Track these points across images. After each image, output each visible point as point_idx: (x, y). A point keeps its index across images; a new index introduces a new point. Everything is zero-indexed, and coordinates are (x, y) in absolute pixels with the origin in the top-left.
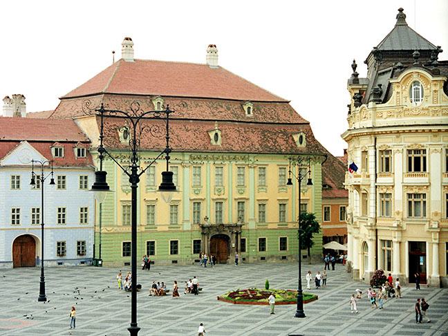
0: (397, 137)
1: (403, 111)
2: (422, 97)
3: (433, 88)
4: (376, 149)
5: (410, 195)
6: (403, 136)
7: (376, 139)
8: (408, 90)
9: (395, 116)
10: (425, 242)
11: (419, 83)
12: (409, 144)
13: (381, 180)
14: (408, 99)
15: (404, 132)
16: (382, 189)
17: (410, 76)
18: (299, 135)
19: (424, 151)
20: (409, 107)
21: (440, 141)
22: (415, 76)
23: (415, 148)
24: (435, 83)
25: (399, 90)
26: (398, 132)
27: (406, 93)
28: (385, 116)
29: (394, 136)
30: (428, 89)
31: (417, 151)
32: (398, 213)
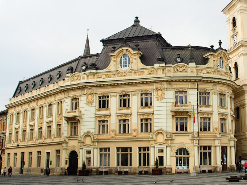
1: (215, 70)
4: (197, 90)
5: (220, 118)
6: (217, 85)
7: (197, 84)
9: (212, 73)
10: (226, 147)
13: (200, 109)
20: (219, 70)
23: (223, 93)
28: (204, 71)
29: (212, 84)
30: (225, 63)
32: (216, 129)
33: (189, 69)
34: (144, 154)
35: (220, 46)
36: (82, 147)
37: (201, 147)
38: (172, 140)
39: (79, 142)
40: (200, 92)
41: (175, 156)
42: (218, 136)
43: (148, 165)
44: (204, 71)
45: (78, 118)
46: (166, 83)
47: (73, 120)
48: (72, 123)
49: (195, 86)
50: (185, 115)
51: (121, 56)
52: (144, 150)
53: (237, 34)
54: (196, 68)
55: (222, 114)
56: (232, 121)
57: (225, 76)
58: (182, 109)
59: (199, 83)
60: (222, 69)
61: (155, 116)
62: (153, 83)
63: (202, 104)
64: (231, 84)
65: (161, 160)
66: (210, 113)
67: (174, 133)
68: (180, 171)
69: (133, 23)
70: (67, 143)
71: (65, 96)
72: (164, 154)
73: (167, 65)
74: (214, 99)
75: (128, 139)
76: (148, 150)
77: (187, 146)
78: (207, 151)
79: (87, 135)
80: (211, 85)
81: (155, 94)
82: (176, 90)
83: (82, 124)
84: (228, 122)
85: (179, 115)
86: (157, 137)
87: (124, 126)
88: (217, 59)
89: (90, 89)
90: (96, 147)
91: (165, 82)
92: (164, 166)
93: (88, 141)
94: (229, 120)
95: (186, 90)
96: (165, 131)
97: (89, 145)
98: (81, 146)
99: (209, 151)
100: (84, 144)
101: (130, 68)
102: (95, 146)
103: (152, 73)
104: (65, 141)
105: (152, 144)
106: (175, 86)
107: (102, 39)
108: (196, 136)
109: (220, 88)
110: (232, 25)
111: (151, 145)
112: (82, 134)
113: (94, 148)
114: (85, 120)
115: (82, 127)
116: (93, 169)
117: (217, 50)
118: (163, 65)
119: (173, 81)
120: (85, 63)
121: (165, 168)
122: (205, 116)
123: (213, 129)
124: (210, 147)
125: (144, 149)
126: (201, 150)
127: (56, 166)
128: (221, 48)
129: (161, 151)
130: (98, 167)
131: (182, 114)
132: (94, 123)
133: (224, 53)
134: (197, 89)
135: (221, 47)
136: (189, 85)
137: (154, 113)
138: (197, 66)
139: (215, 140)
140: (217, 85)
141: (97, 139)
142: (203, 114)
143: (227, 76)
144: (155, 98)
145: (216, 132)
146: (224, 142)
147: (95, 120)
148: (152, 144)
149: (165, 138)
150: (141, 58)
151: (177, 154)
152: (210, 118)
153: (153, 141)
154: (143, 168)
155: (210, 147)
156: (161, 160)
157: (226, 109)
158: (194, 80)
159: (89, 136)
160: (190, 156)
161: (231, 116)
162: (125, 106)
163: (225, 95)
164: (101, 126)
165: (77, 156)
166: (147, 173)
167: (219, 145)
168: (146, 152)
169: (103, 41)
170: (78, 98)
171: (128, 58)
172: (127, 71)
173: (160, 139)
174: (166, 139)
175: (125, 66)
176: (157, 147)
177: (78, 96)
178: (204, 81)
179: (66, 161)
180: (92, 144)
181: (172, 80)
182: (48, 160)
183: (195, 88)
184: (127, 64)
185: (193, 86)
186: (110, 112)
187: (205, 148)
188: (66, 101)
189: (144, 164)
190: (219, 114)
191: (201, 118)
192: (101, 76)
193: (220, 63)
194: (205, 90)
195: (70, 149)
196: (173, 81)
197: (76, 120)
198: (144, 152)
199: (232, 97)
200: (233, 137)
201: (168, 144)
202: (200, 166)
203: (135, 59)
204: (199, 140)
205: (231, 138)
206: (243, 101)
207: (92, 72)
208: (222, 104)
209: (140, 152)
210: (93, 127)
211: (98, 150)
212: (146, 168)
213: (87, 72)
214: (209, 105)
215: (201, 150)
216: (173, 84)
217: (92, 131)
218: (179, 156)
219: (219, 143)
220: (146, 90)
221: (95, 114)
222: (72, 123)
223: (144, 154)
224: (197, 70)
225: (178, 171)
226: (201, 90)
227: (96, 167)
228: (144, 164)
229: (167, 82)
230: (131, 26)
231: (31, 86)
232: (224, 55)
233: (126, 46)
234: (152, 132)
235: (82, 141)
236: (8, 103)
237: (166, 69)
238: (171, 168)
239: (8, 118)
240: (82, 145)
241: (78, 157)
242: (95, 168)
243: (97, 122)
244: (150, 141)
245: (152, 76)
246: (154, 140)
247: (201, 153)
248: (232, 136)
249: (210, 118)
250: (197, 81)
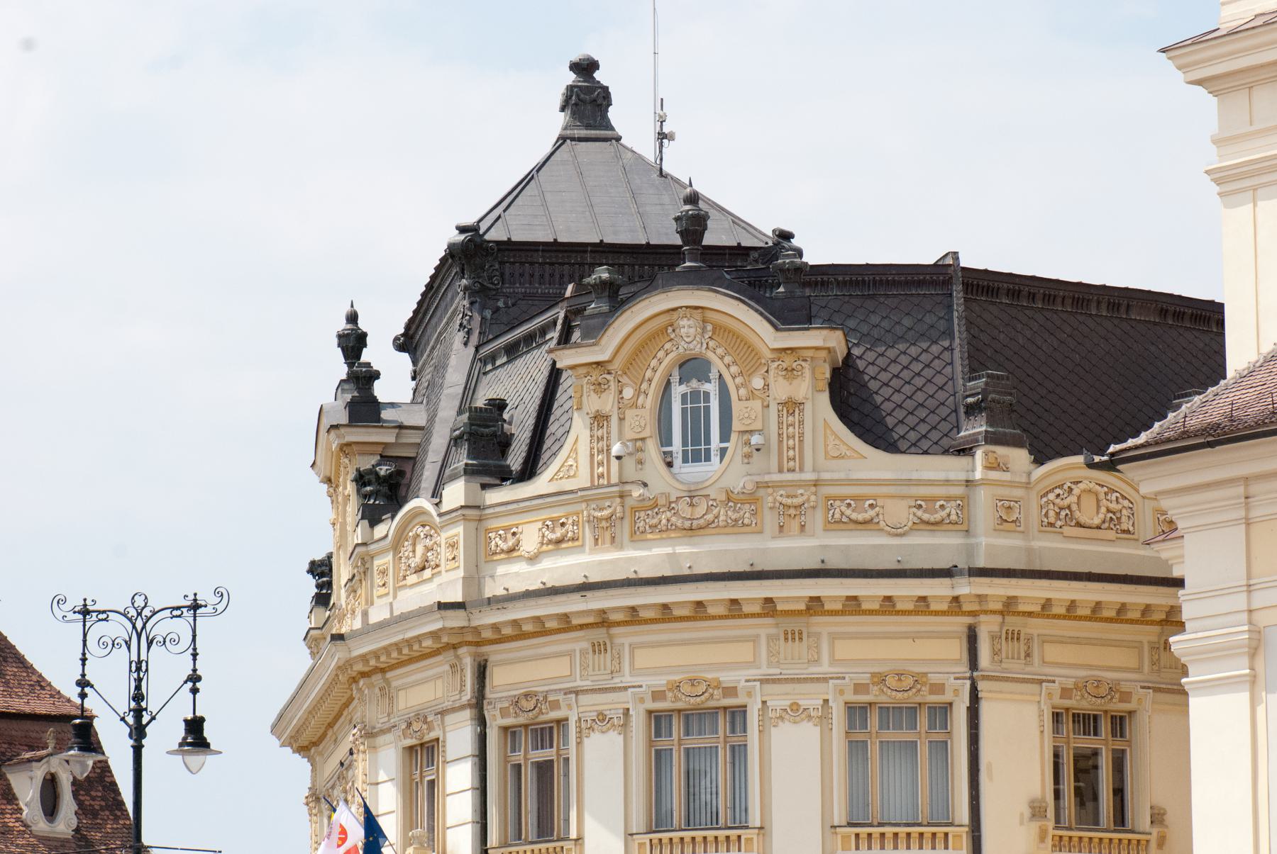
0: (599, 648)
2: (725, 437)
3: (781, 389)
4: (482, 721)
6: (625, 637)
8: (650, 401)
11: (707, 364)
12: (660, 682)
14: (653, 450)
15: (633, 616)
17: (663, 331)
18: (39, 772)
19: (737, 715)
21: (817, 661)
22: (687, 327)
24: (788, 361)
25: (607, 403)
26: (603, 621)
27: (642, 420)
28: (530, 539)
29: (578, 643)
30: (752, 395)
31: (695, 718)
57: (736, 526)
109: (645, 658)
134: (467, 714)
140: (627, 641)
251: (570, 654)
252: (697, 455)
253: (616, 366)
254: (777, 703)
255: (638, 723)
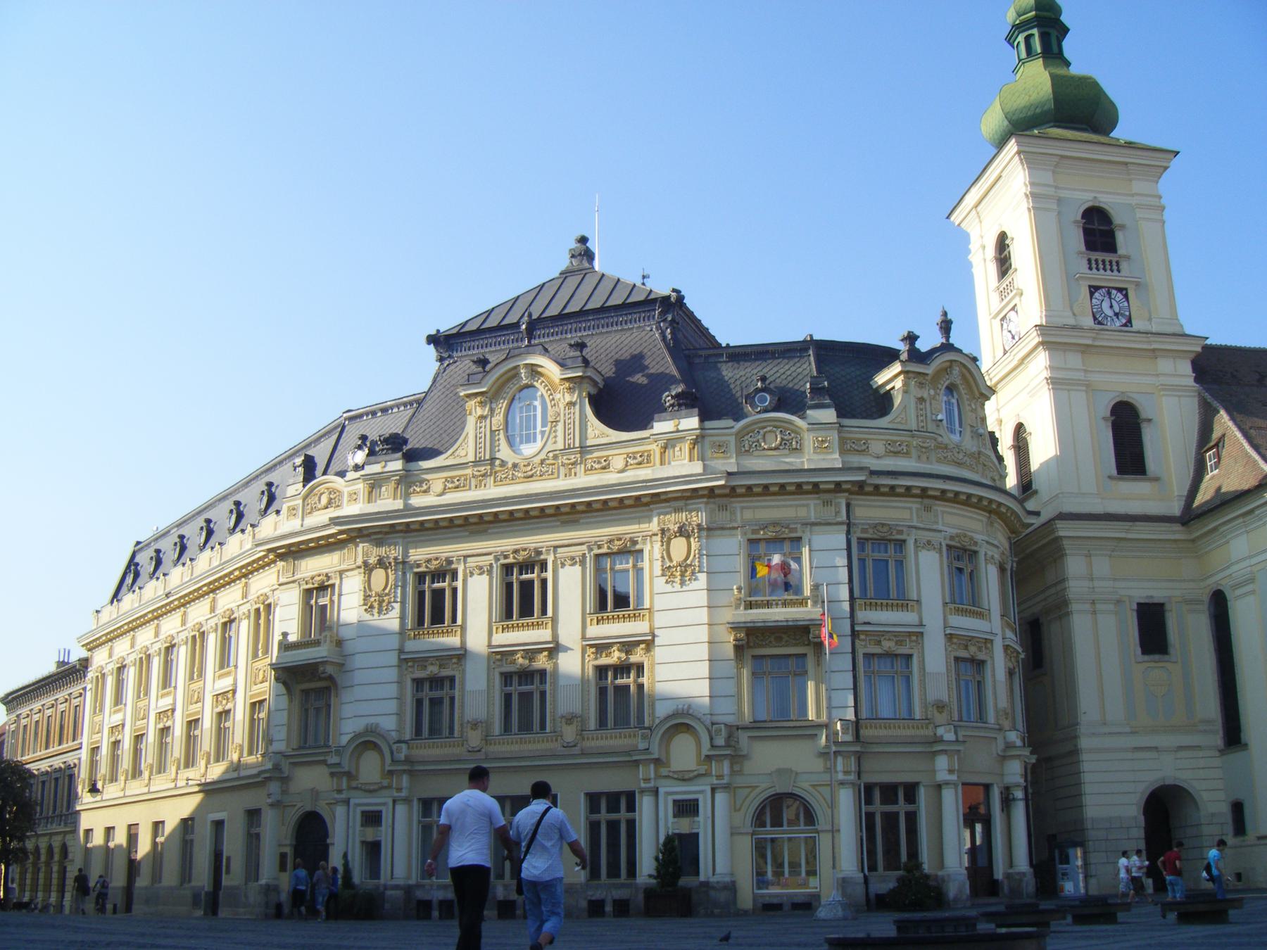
2: (961, 426)
4: (848, 533)
5: (957, 659)
6: (940, 507)
7: (848, 505)
9: (914, 452)
12: (954, 531)
16: (879, 643)
20: (945, 440)
22: (956, 370)
25: (925, 396)
26: (943, 496)
28: (877, 447)
29: (914, 504)
32: (940, 707)
33: (809, 440)
34: (613, 826)
35: (948, 338)
36: (343, 796)
37: (869, 788)
38: (737, 758)
39: (332, 774)
40: (862, 542)
41: (750, 830)
42: (950, 736)
43: (632, 872)
44: (877, 447)
45: (330, 670)
46: (707, 503)
47: (310, 681)
48: (306, 693)
49: (837, 513)
50: (796, 645)
51: (509, 396)
52: (613, 807)
53: (1016, 301)
54: (839, 432)
55: (966, 641)
56: (1011, 673)
57: (971, 468)
58: (778, 614)
59: (857, 501)
60: (956, 438)
61: (659, 653)
62: (647, 504)
63: (871, 593)
64: (1000, 504)
65: (680, 853)
66: (910, 634)
67: (745, 728)
68: (775, 901)
69: (564, 262)
70: (285, 780)
71: (282, 580)
72: (701, 824)
73: (708, 424)
74: (928, 573)
75: (541, 757)
76: (631, 807)
77: (806, 785)
78: (901, 807)
79: (368, 742)
80: (910, 509)
81: (657, 555)
82: (754, 532)
83: (347, 696)
84: (994, 675)
85: (769, 645)
86: (668, 745)
87: (526, 697)
88: (932, 392)
89: (379, 543)
90: (404, 794)
91: (703, 496)
92: (702, 878)
93: (370, 768)
94: (999, 665)
95: (795, 530)
96: (704, 718)
97: (376, 787)
98: (340, 791)
99: (910, 808)
100: (354, 784)
101: (550, 447)
102: (399, 790)
103: (645, 460)
104: (277, 767)
105: (647, 780)
106: (748, 515)
107: (434, 332)
108: (849, 738)
110: (992, 268)
111: (643, 785)
112: (344, 740)
113: (394, 801)
114: (359, 677)
115: (347, 710)
116: (389, 893)
117: (933, 351)
118: (691, 422)
119: (739, 491)
120: (364, 438)
121: (706, 884)
122: (888, 645)
123: (925, 705)
124: (911, 791)
125: (614, 800)
126: (869, 801)
127: (247, 880)
128: (947, 347)
129: (686, 808)
130: (412, 882)
131: (779, 639)
132: (393, 690)
133: (964, 366)
134: (845, 527)
135: (951, 341)
136: (809, 508)
137: (653, 641)
138: (847, 422)
139: (935, 753)
141: (408, 760)
142: (877, 637)
143: (980, 467)
144: (658, 571)
145: (940, 718)
146: (982, 764)
147: (401, 675)
148: (647, 780)
149: (706, 750)
150: (590, 397)
151: (759, 820)
152: (911, 656)
153: (652, 766)
154: (608, 891)
155: (911, 791)
156: (680, 853)
157: (980, 615)
158: (832, 486)
159: (375, 746)
160: (818, 832)
161: (1006, 647)
162: (526, 611)
163: (976, 552)
164: (426, 704)
165: (326, 835)
166: (622, 908)
167: (954, 777)
168: (623, 815)
169: (433, 340)
170: (333, 586)
171: (537, 403)
172: (537, 460)
173: (684, 753)
174: (707, 756)
175: (530, 439)
176: (672, 791)
177: (328, 578)
178: (877, 487)
179: (283, 856)
180: (385, 783)
181: (733, 488)
182: (217, 855)
183: (839, 519)
184: (535, 428)
185: (828, 514)
186: (463, 642)
187: (889, 792)
188: (280, 603)
189: (614, 871)
190: (950, 637)
191: (868, 656)
192: (425, 487)
193: (949, 413)
194: (885, 529)
195: (299, 805)
196: (739, 491)
197: (321, 679)
198: (614, 816)
199: (1008, 567)
200: (1019, 743)
201: (720, 777)
202: (866, 878)
203: (572, 404)
204: (859, 757)
205: (1009, 746)
206: (1059, 588)
207: (387, 469)
208: (963, 594)
209: (595, 817)
210: (392, 706)
211: (411, 808)
212: (623, 886)
213: (370, 469)
214: (903, 602)
215: (869, 801)
216: (737, 504)
217: (388, 724)
218: (769, 832)
219: (951, 771)
220: (620, 539)
221: (401, 651)
222: (306, 693)
223: (613, 826)
224: (843, 441)
225: (767, 900)
226: (864, 531)
227: (401, 882)
228: (614, 871)
229: (709, 497)
230: (557, 275)
231: (170, 554)
232: (964, 377)
233: (530, 348)
234: (646, 724)
235: (346, 769)
236: (88, 625)
237: (708, 440)
238: (731, 887)
239: (89, 687)
240: (344, 786)
241: (329, 841)
242: (396, 887)
243: (409, 683)
244: (636, 763)
245: (644, 473)
246: (657, 762)
247: (870, 817)
248: (1013, 737)
249: (911, 656)
250: (844, 486)
251: (910, 509)
252: (952, 431)
253: (929, 378)
254: (990, 553)
255: (944, 548)
